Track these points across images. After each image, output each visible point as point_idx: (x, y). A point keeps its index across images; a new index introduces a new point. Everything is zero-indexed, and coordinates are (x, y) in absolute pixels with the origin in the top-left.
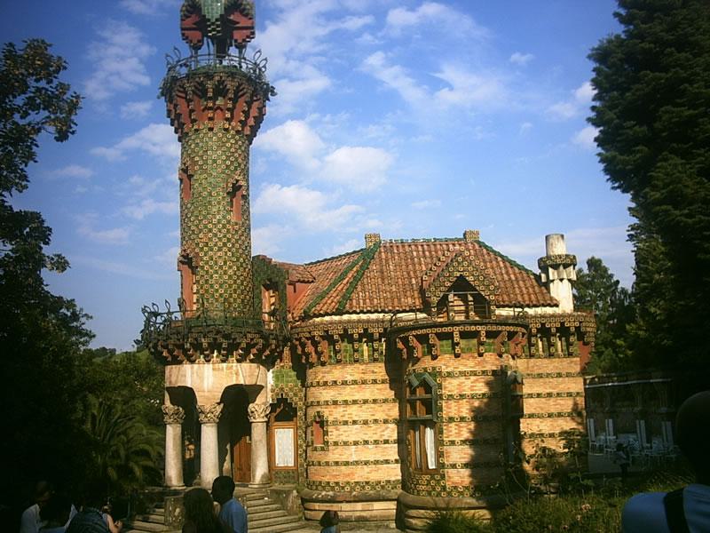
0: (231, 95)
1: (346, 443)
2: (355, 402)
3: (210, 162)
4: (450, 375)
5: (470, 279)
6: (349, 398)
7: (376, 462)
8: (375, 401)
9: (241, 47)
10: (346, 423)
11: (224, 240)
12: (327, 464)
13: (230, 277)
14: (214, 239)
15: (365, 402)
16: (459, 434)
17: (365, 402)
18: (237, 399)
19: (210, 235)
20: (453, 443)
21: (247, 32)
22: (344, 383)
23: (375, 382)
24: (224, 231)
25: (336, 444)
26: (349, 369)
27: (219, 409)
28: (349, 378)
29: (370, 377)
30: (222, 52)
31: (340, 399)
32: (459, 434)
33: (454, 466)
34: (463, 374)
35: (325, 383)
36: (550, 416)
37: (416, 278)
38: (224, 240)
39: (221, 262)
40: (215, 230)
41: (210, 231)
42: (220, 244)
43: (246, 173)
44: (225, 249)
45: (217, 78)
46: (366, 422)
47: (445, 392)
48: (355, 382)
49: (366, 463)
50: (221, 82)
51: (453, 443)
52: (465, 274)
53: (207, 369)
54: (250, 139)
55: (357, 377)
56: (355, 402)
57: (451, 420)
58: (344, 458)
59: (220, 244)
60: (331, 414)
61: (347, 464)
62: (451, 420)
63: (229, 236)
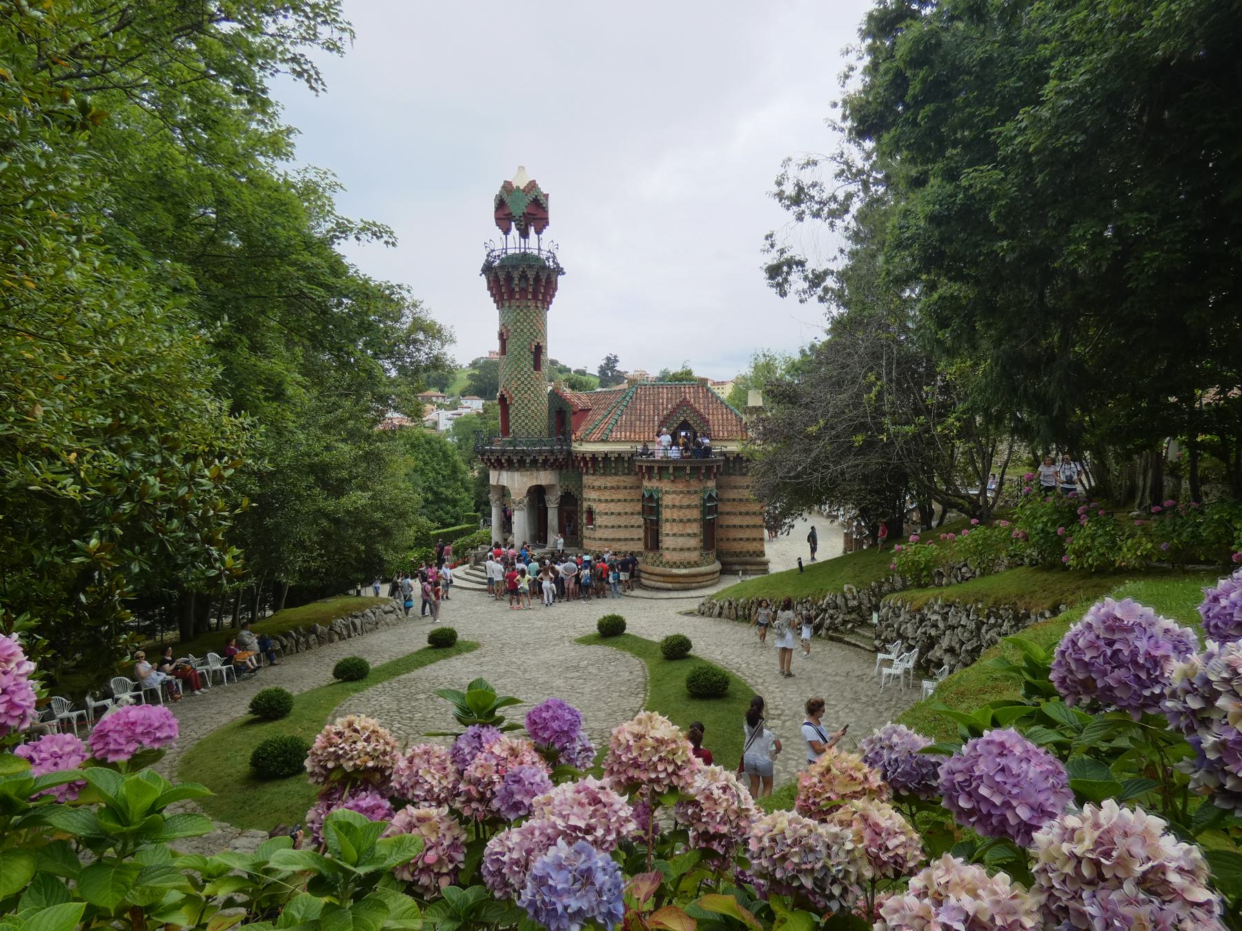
0: (531, 283)
1: (606, 527)
2: (612, 501)
3: (519, 330)
4: (667, 492)
5: (691, 422)
6: (609, 498)
7: (626, 540)
8: (625, 500)
9: (538, 232)
10: (606, 514)
11: (529, 386)
12: (594, 539)
13: (533, 411)
14: (522, 386)
15: (619, 501)
16: (672, 529)
17: (619, 501)
18: (537, 495)
19: (519, 382)
20: (668, 535)
21: (543, 222)
22: (605, 488)
23: (625, 488)
24: (529, 379)
25: (600, 526)
26: (609, 478)
27: (526, 501)
28: (609, 484)
29: (622, 484)
30: (524, 234)
31: (603, 498)
32: (672, 529)
33: (667, 549)
34: (674, 492)
35: (593, 487)
36: (741, 514)
37: (658, 415)
38: (529, 386)
39: (526, 402)
40: (522, 379)
41: (519, 379)
42: (526, 389)
43: (544, 336)
44: (529, 392)
45: (521, 269)
46: (619, 514)
47: (664, 503)
48: (612, 488)
49: (619, 540)
50: (524, 272)
51: (668, 535)
52: (688, 419)
53: (517, 475)
54: (548, 309)
55: (614, 484)
56: (612, 501)
57: (667, 520)
58: (605, 536)
59: (526, 389)
60: (597, 507)
61: (606, 540)
62: (667, 520)
63: (532, 382)
